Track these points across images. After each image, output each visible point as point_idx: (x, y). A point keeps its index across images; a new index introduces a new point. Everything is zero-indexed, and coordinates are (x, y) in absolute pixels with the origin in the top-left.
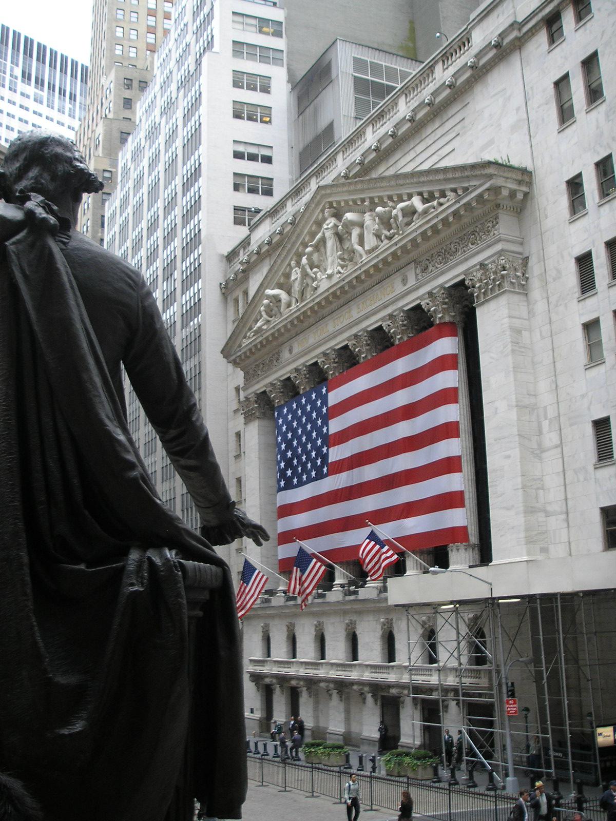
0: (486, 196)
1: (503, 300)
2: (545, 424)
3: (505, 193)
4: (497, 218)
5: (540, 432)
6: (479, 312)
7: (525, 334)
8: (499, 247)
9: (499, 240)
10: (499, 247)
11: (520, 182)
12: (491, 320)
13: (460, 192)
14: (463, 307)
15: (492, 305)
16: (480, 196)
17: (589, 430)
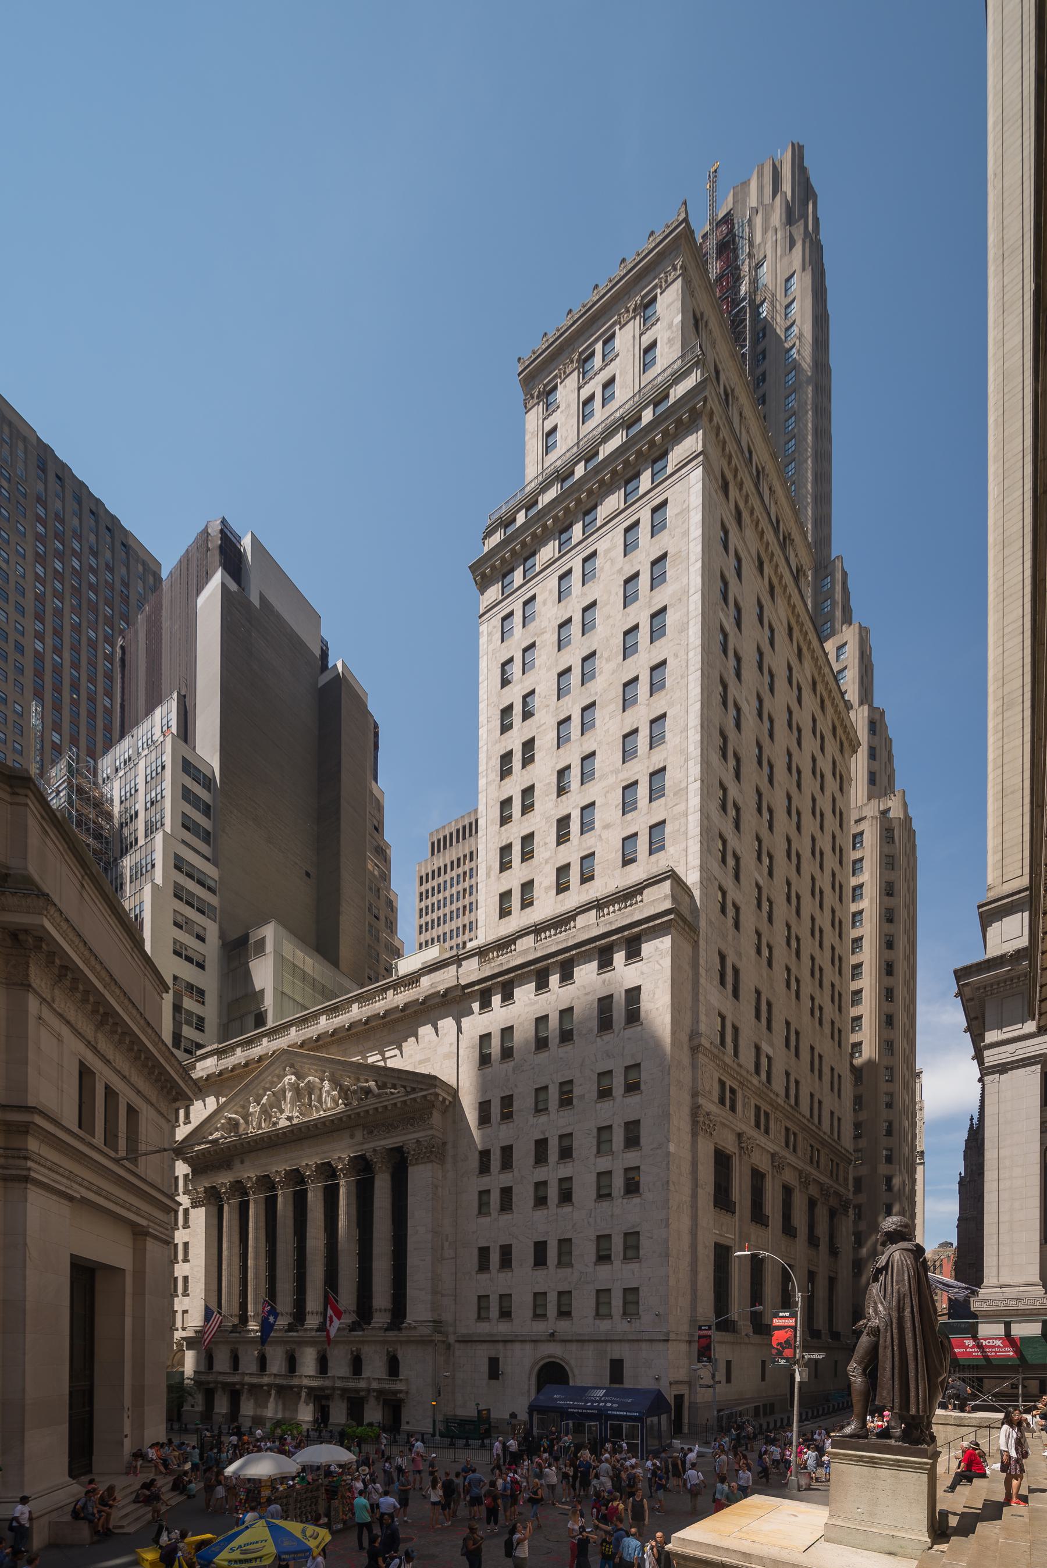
0: (429, 1098)
1: (429, 1166)
2: (446, 1245)
3: (441, 1099)
4: (431, 1113)
5: (443, 1248)
6: (410, 1169)
7: (440, 1189)
8: (430, 1132)
9: (432, 1128)
10: (430, 1132)
11: (449, 1094)
12: (419, 1176)
13: (409, 1089)
14: (399, 1164)
15: (421, 1167)
16: (425, 1096)
17: (476, 1252)
